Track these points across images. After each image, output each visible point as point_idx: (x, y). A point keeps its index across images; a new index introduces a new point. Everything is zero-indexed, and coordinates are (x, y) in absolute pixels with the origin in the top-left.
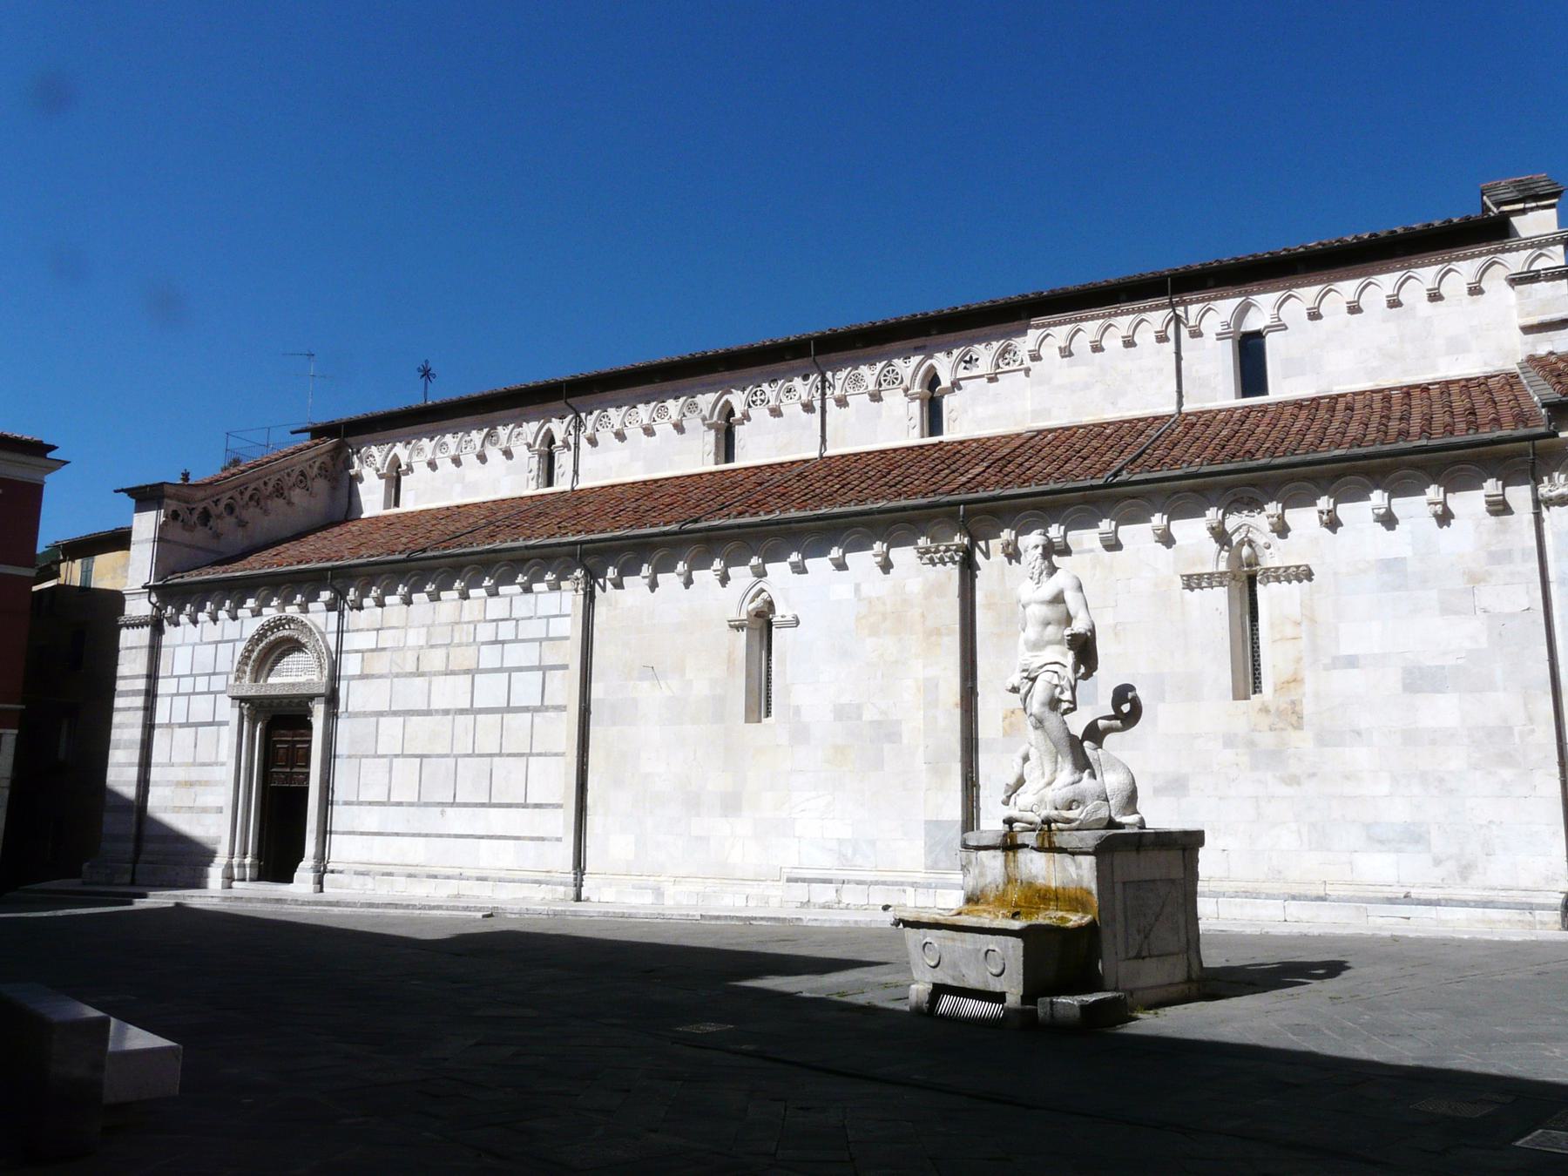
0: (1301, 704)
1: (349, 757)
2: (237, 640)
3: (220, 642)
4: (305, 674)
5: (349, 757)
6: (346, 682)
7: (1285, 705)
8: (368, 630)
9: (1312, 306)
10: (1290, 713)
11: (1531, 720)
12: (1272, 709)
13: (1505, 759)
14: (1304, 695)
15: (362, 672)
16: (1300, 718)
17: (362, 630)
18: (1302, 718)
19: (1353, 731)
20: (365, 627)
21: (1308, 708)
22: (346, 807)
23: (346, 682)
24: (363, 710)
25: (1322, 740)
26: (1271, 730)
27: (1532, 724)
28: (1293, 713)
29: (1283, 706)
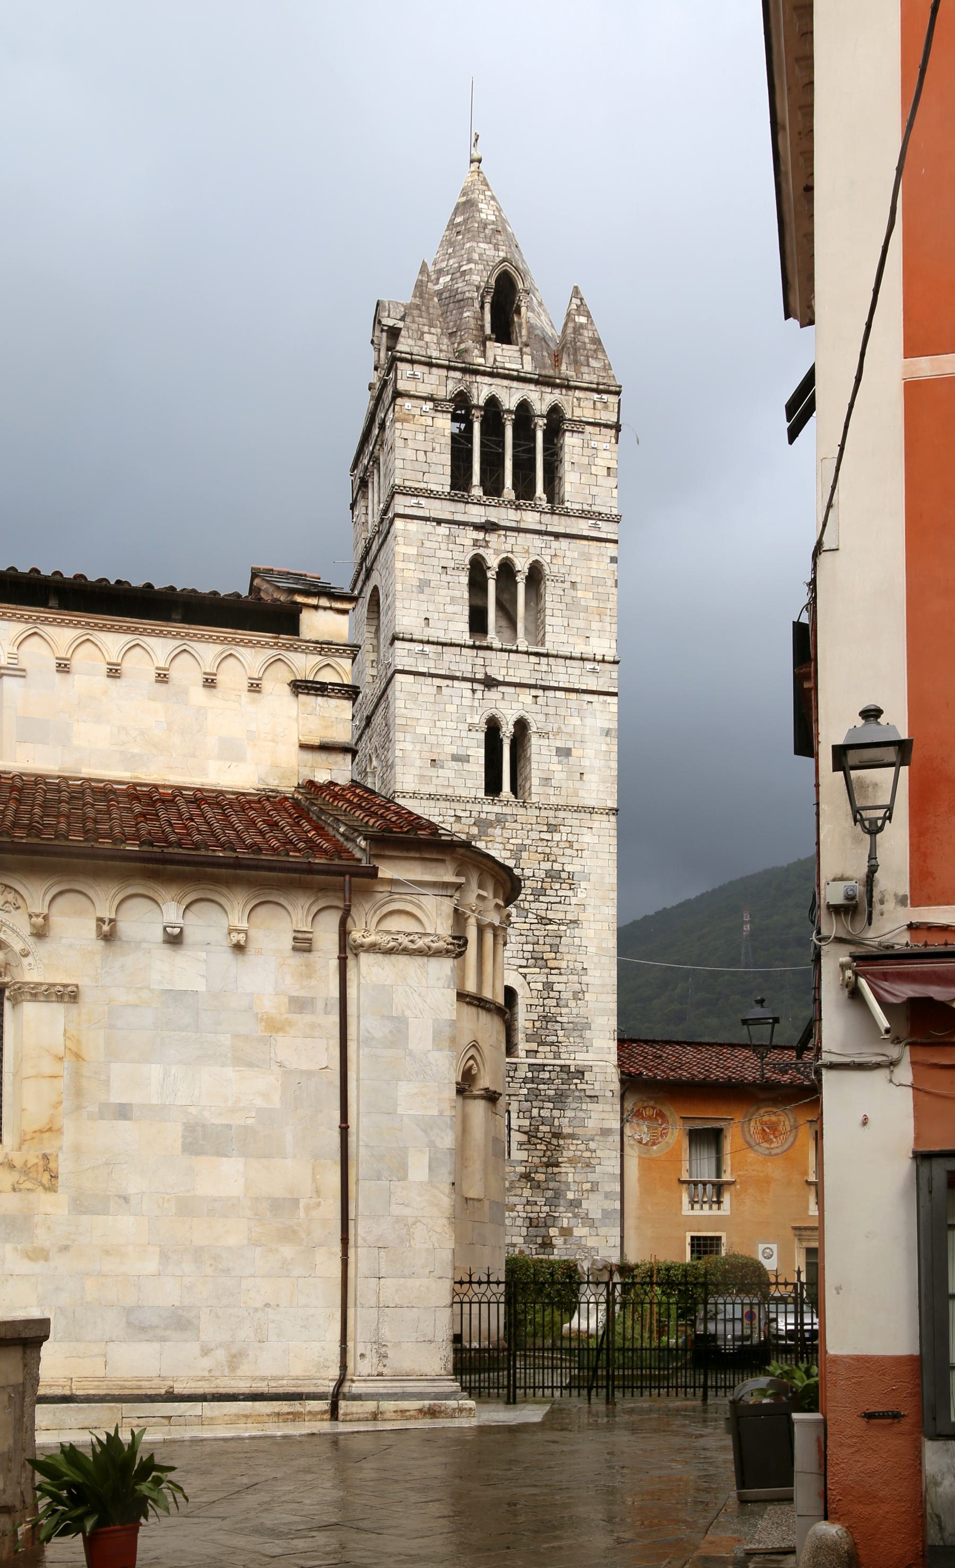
0: (56, 1161)
7: (36, 1161)
9: (64, 656)
10: (41, 1169)
11: (318, 1192)
12: (18, 1163)
13: (288, 1235)
14: (60, 1148)
16: (54, 1177)
18: (56, 1177)
19: (120, 1197)
21: (64, 1166)
25: (80, 1205)
26: (14, 1190)
27: (319, 1196)
28: (44, 1171)
29: (32, 1161)
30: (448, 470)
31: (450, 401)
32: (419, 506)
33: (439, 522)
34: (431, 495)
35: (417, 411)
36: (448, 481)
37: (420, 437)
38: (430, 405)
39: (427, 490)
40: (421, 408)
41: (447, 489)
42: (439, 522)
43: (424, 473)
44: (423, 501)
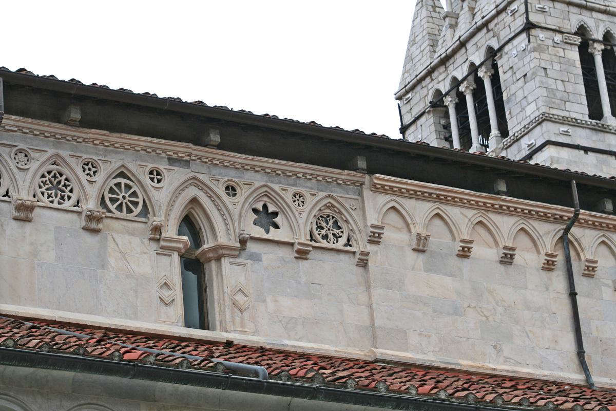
30: (584, 100)
31: (575, 34)
32: (566, 134)
33: (586, 150)
34: (575, 123)
35: (550, 43)
36: (587, 112)
37: (557, 67)
38: (558, 38)
39: (572, 119)
40: (553, 40)
41: (587, 118)
42: (586, 150)
43: (565, 102)
44: (571, 130)
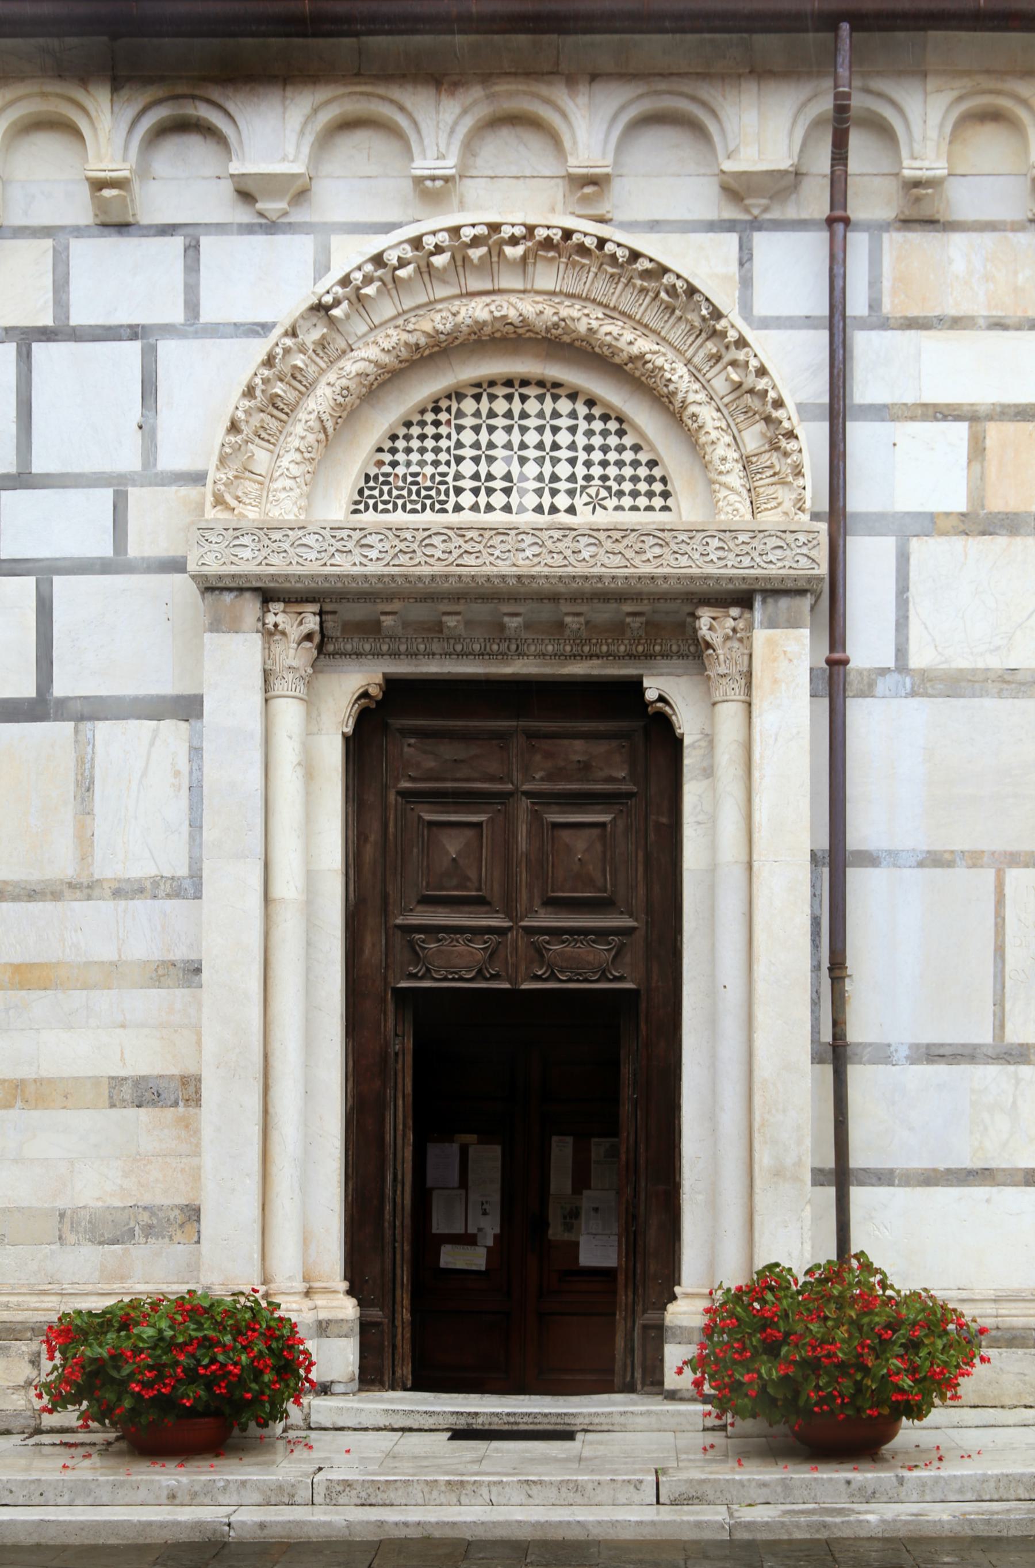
1: (935, 860)
2: (168, 330)
3: (47, 334)
4: (596, 504)
5: (935, 860)
6: (888, 544)
8: (999, 325)
15: (977, 492)
17: (957, 323)
20: (978, 307)
22: (941, 1071)
23: (888, 544)
24: (996, 663)
